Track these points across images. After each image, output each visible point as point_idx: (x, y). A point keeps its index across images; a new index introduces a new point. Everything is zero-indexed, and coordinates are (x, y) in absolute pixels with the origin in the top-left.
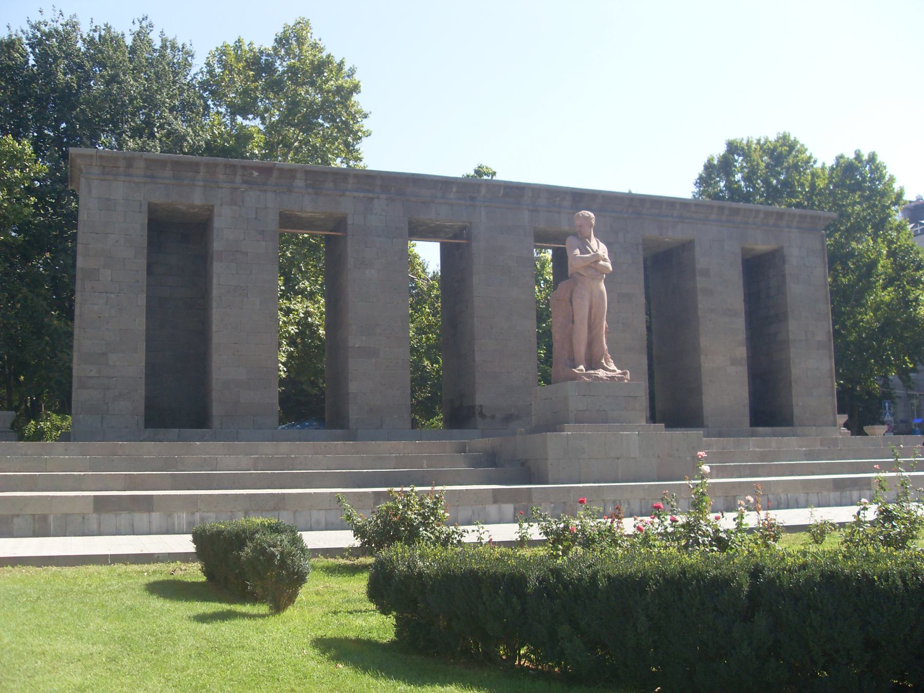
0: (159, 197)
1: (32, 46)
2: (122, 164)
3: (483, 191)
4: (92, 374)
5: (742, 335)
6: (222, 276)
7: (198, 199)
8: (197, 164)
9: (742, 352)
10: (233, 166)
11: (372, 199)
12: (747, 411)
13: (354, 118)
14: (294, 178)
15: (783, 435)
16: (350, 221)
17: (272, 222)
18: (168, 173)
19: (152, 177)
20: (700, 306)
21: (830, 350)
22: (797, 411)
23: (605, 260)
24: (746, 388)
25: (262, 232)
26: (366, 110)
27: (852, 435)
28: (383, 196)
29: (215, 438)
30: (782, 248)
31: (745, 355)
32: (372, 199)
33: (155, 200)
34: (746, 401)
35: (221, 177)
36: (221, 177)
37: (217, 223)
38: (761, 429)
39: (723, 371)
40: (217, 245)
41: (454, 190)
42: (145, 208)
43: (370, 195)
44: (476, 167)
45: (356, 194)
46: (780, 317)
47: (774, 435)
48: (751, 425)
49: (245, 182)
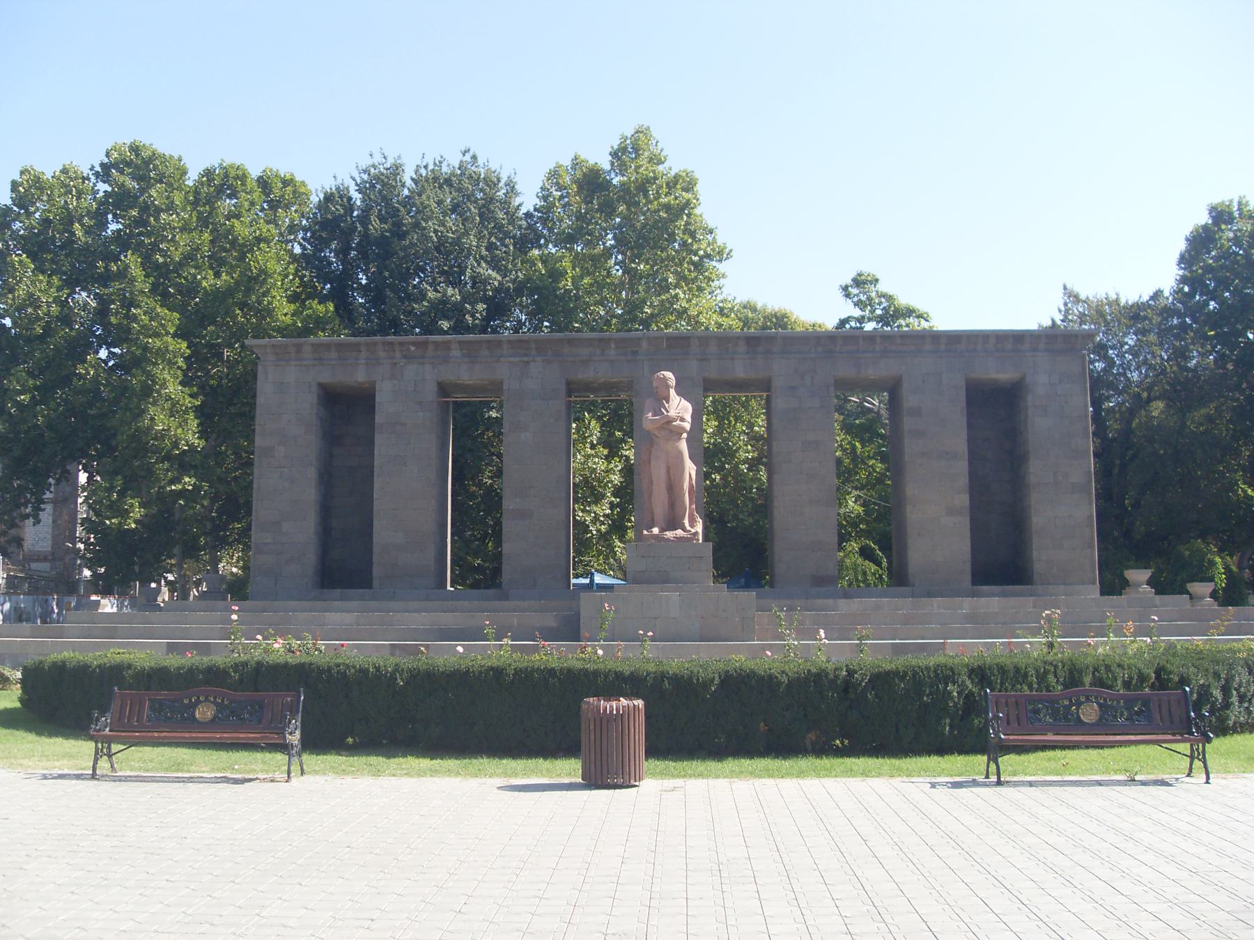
0: (327, 377)
1: (360, 191)
3: (644, 344)
5: (963, 481)
6: (383, 447)
7: (360, 376)
8: (358, 345)
9: (963, 500)
10: (391, 343)
11: (528, 362)
12: (968, 568)
13: (693, 235)
14: (449, 349)
15: (1014, 595)
16: (505, 387)
17: (430, 392)
18: (334, 355)
19: (320, 359)
20: (907, 450)
21: (1090, 494)
23: (682, 420)
24: (968, 541)
25: (420, 403)
26: (711, 225)
27: (1156, 593)
28: (539, 359)
31: (967, 503)
32: (528, 362)
33: (323, 381)
34: (968, 556)
36: (382, 354)
37: (382, 397)
38: (985, 588)
39: (939, 520)
40: (378, 419)
41: (613, 346)
42: (315, 388)
43: (526, 359)
44: (853, 274)
45: (512, 359)
47: (1005, 595)
48: (974, 583)
49: (404, 357)
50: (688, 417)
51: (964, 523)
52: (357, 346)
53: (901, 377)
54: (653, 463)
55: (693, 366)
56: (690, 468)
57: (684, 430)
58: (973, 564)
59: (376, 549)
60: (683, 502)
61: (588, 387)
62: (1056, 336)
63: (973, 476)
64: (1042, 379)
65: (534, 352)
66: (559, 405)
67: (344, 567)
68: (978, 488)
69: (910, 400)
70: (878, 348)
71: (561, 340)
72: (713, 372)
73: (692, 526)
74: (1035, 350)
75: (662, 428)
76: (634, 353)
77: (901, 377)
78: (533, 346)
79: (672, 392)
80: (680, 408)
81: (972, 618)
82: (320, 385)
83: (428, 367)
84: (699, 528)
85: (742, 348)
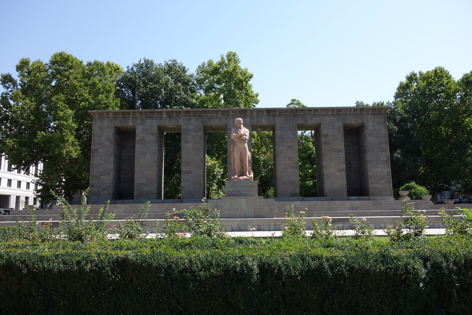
0: (118, 124)
2: (105, 114)
3: (231, 113)
4: (96, 183)
5: (343, 160)
7: (131, 124)
8: (129, 113)
9: (343, 166)
12: (346, 190)
16: (182, 128)
18: (121, 116)
22: (371, 190)
23: (246, 135)
29: (134, 203)
30: (363, 123)
31: (345, 167)
32: (190, 119)
33: (116, 125)
34: (346, 186)
35: (138, 116)
36: (138, 116)
37: (137, 132)
42: (113, 128)
46: (365, 151)
47: (359, 200)
49: (146, 117)
50: (248, 135)
51: (344, 174)
52: (129, 113)
53: (320, 124)
54: (235, 151)
55: (248, 120)
56: (249, 154)
57: (246, 138)
58: (347, 189)
59: (135, 185)
60: (246, 166)
61: (211, 128)
62: (375, 109)
63: (346, 159)
64: (370, 124)
65: (192, 116)
66: (201, 134)
67: (124, 192)
68: (348, 163)
69: (324, 131)
70: (312, 113)
71: (202, 111)
72: (255, 123)
73: (249, 174)
74: (368, 114)
75: (238, 138)
76: (228, 116)
77: (320, 124)
78: (192, 113)
79: (242, 125)
80: (245, 131)
81: (353, 208)
82: (116, 127)
83: (155, 121)
84: (252, 175)
85: (265, 114)
